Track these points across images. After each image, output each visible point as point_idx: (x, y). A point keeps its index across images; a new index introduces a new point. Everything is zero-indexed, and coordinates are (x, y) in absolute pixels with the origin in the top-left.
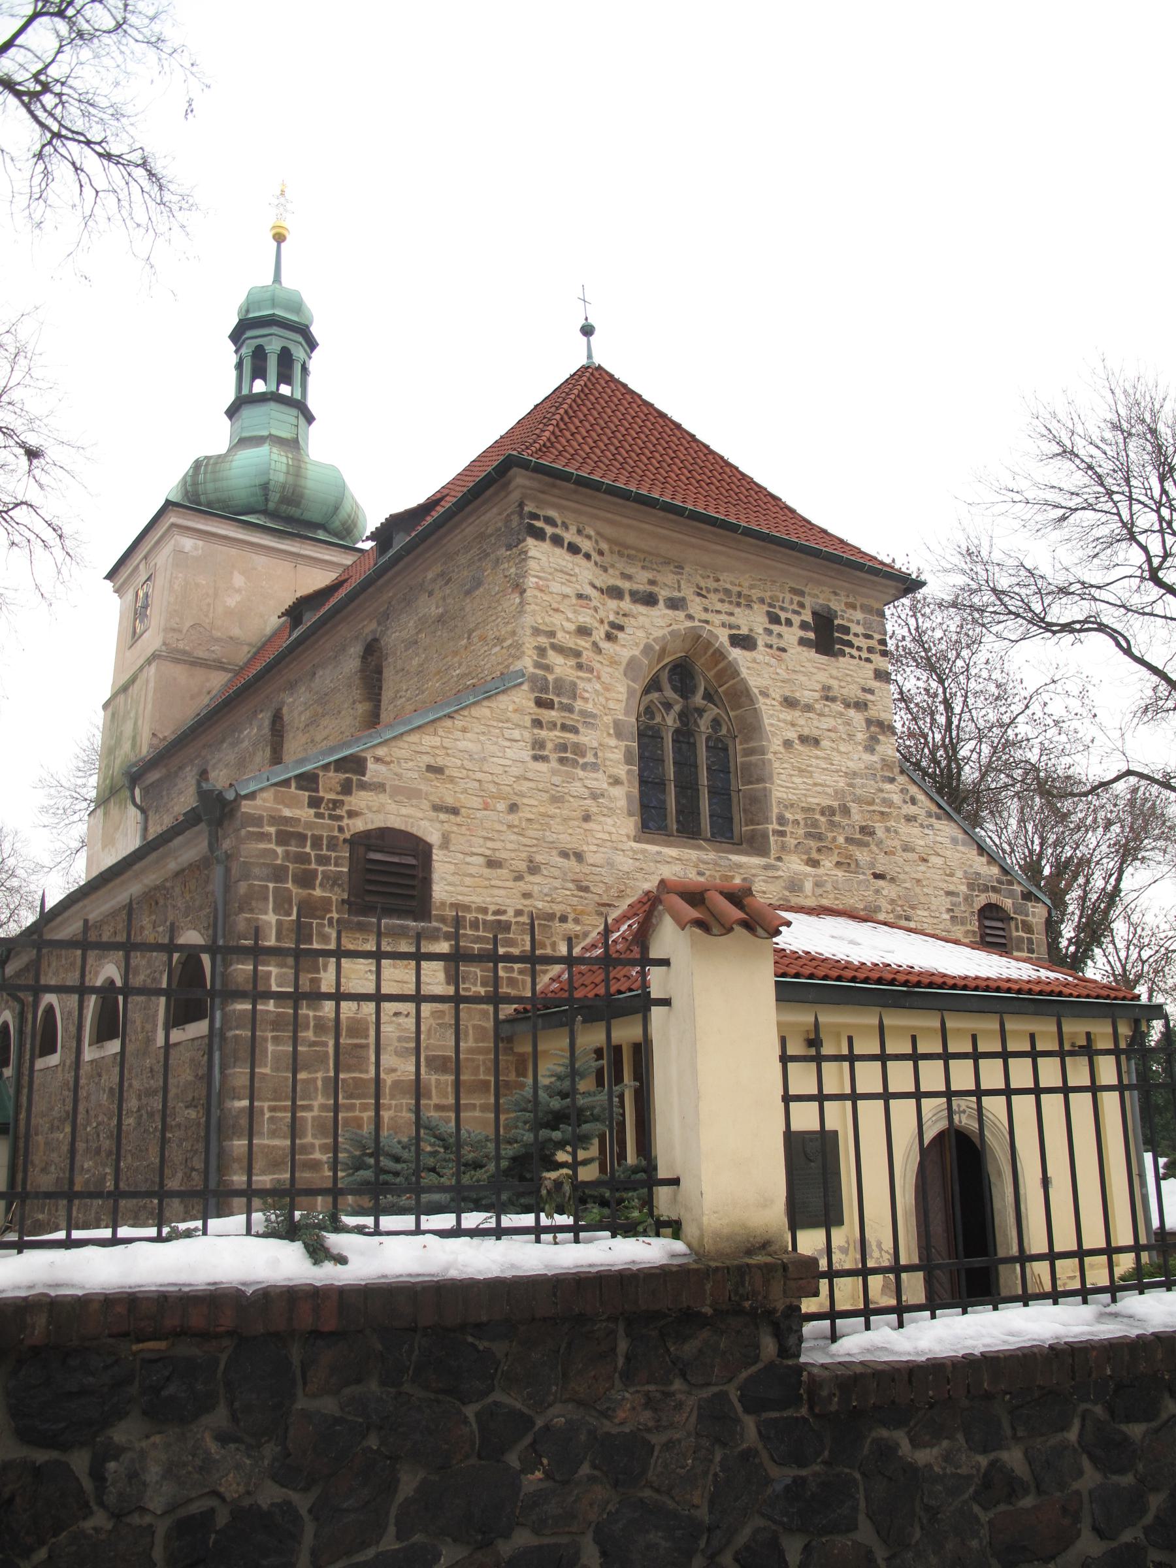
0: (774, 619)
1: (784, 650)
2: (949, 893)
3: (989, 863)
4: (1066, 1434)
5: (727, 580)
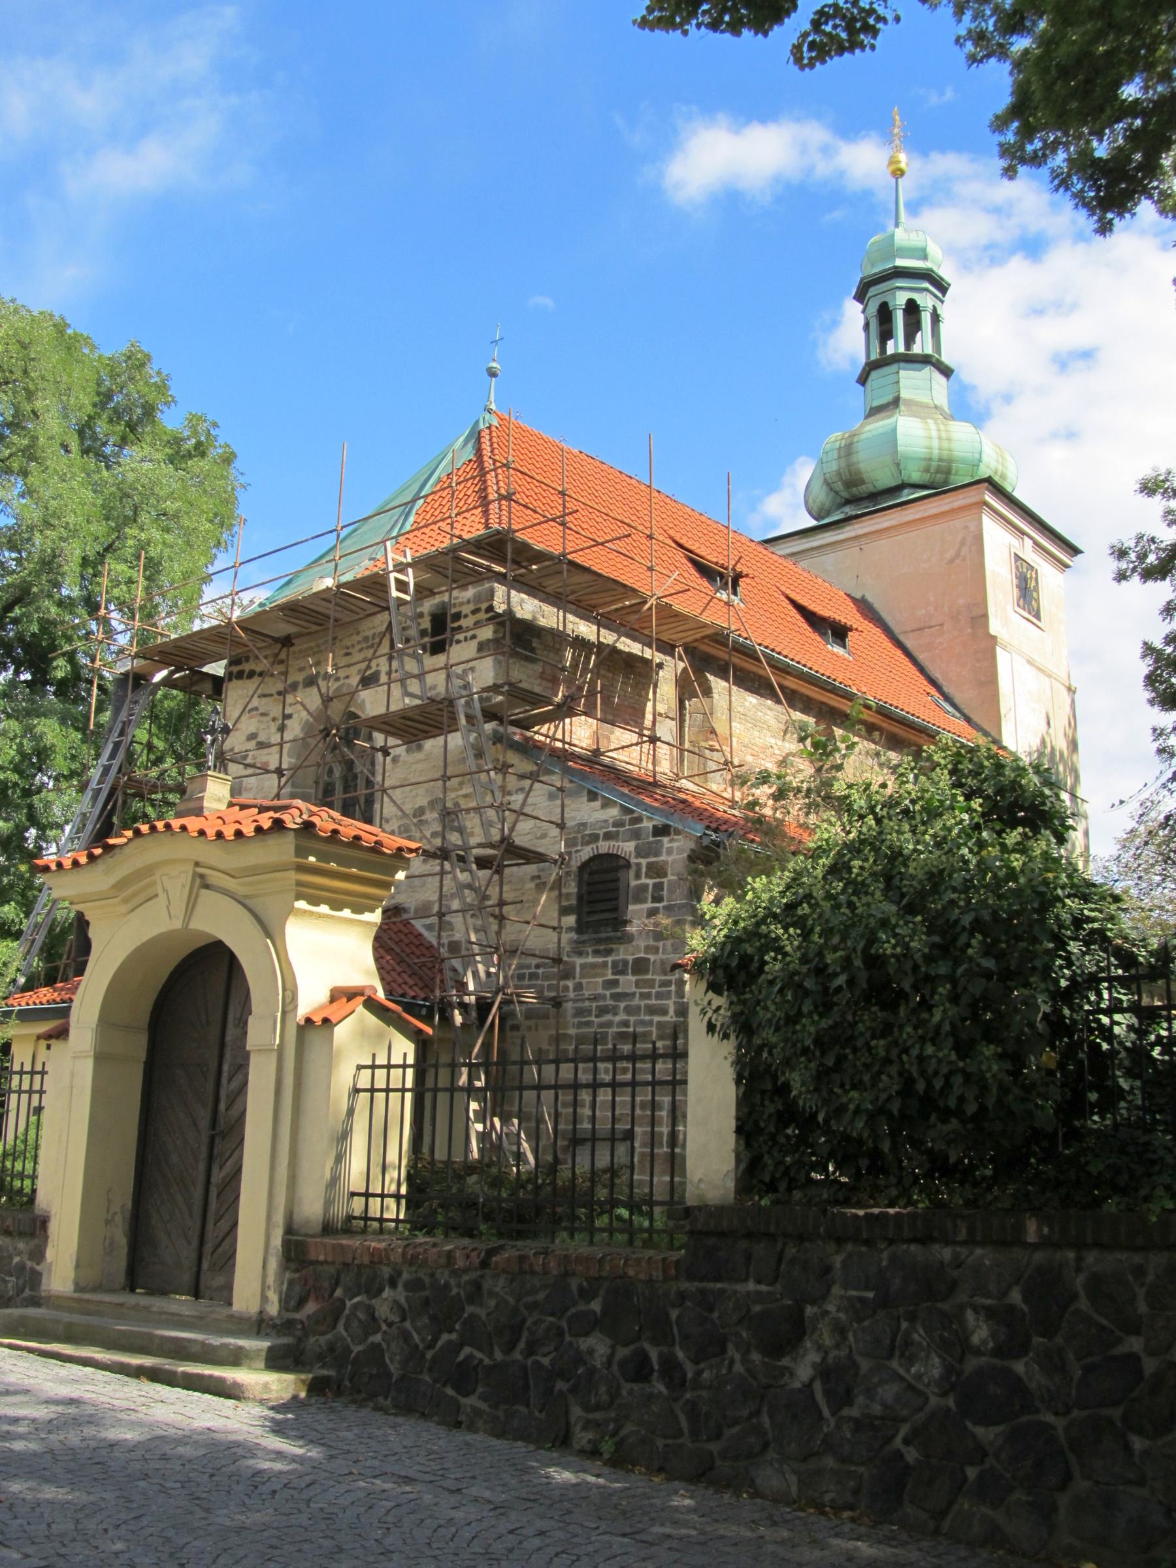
3: (604, 806)
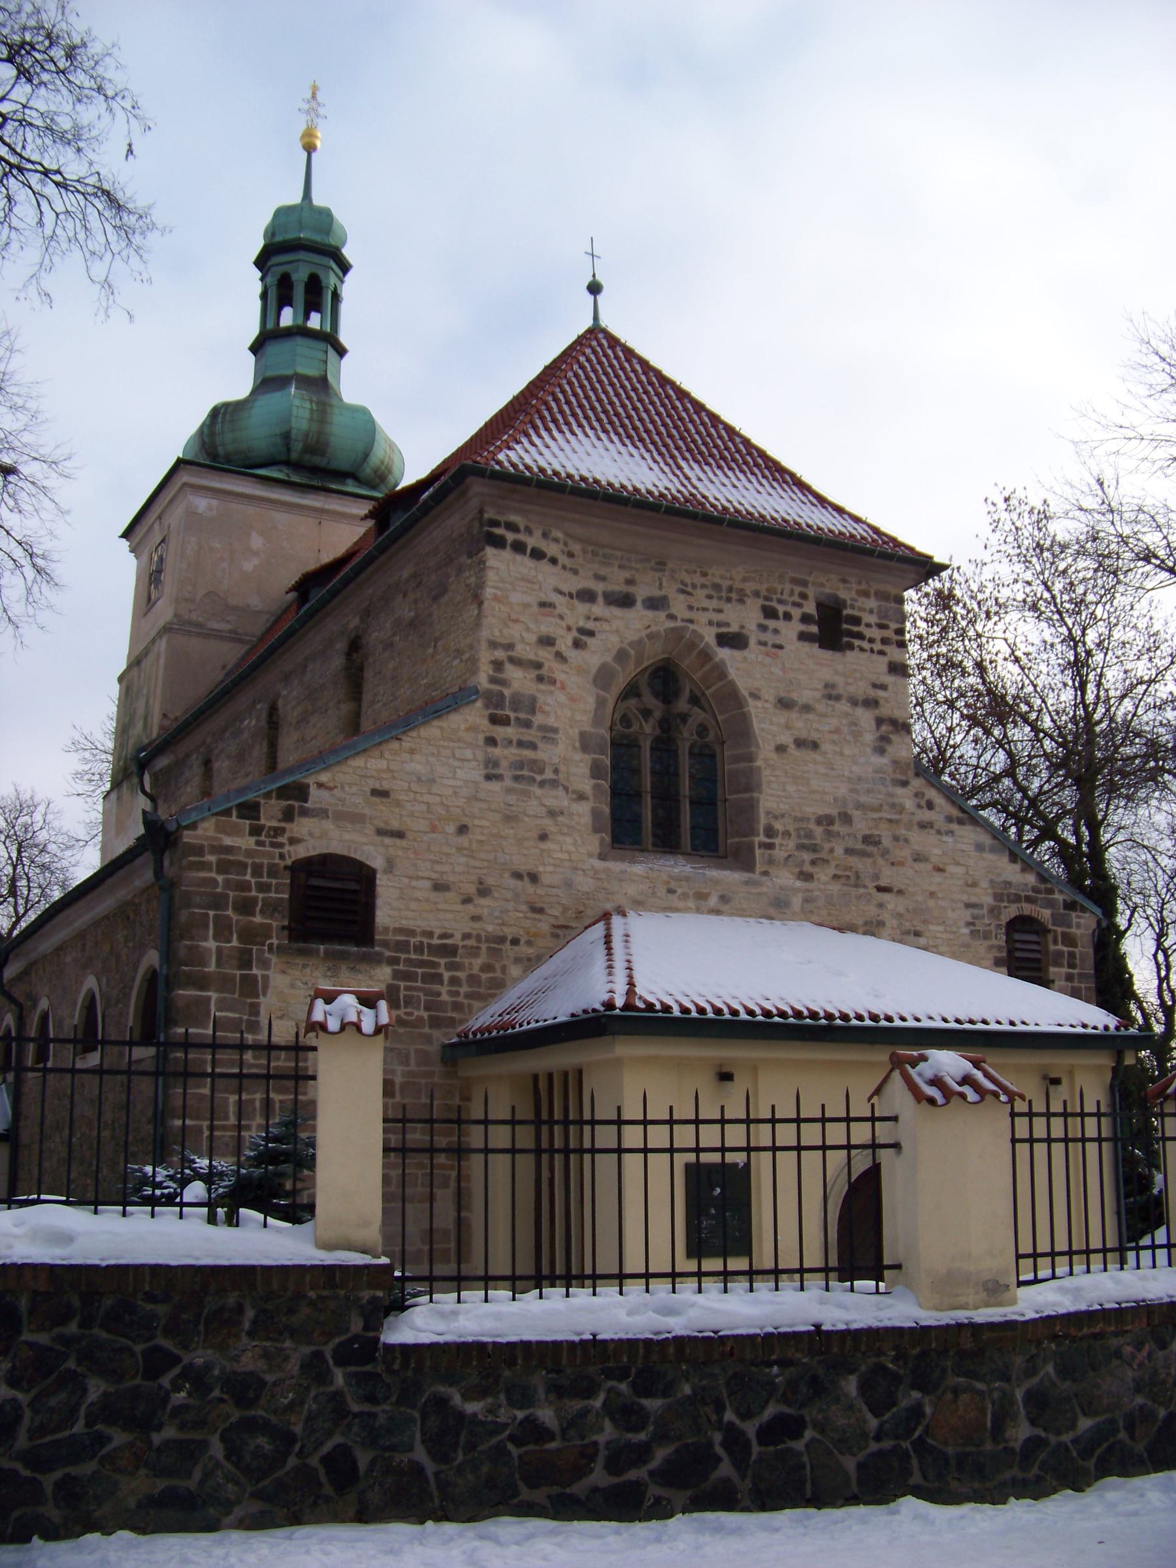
0: (770, 613)
1: (780, 647)
2: (968, 906)
3: (1023, 870)
4: (591, 1402)
5: (716, 574)
